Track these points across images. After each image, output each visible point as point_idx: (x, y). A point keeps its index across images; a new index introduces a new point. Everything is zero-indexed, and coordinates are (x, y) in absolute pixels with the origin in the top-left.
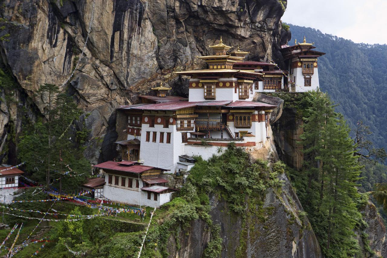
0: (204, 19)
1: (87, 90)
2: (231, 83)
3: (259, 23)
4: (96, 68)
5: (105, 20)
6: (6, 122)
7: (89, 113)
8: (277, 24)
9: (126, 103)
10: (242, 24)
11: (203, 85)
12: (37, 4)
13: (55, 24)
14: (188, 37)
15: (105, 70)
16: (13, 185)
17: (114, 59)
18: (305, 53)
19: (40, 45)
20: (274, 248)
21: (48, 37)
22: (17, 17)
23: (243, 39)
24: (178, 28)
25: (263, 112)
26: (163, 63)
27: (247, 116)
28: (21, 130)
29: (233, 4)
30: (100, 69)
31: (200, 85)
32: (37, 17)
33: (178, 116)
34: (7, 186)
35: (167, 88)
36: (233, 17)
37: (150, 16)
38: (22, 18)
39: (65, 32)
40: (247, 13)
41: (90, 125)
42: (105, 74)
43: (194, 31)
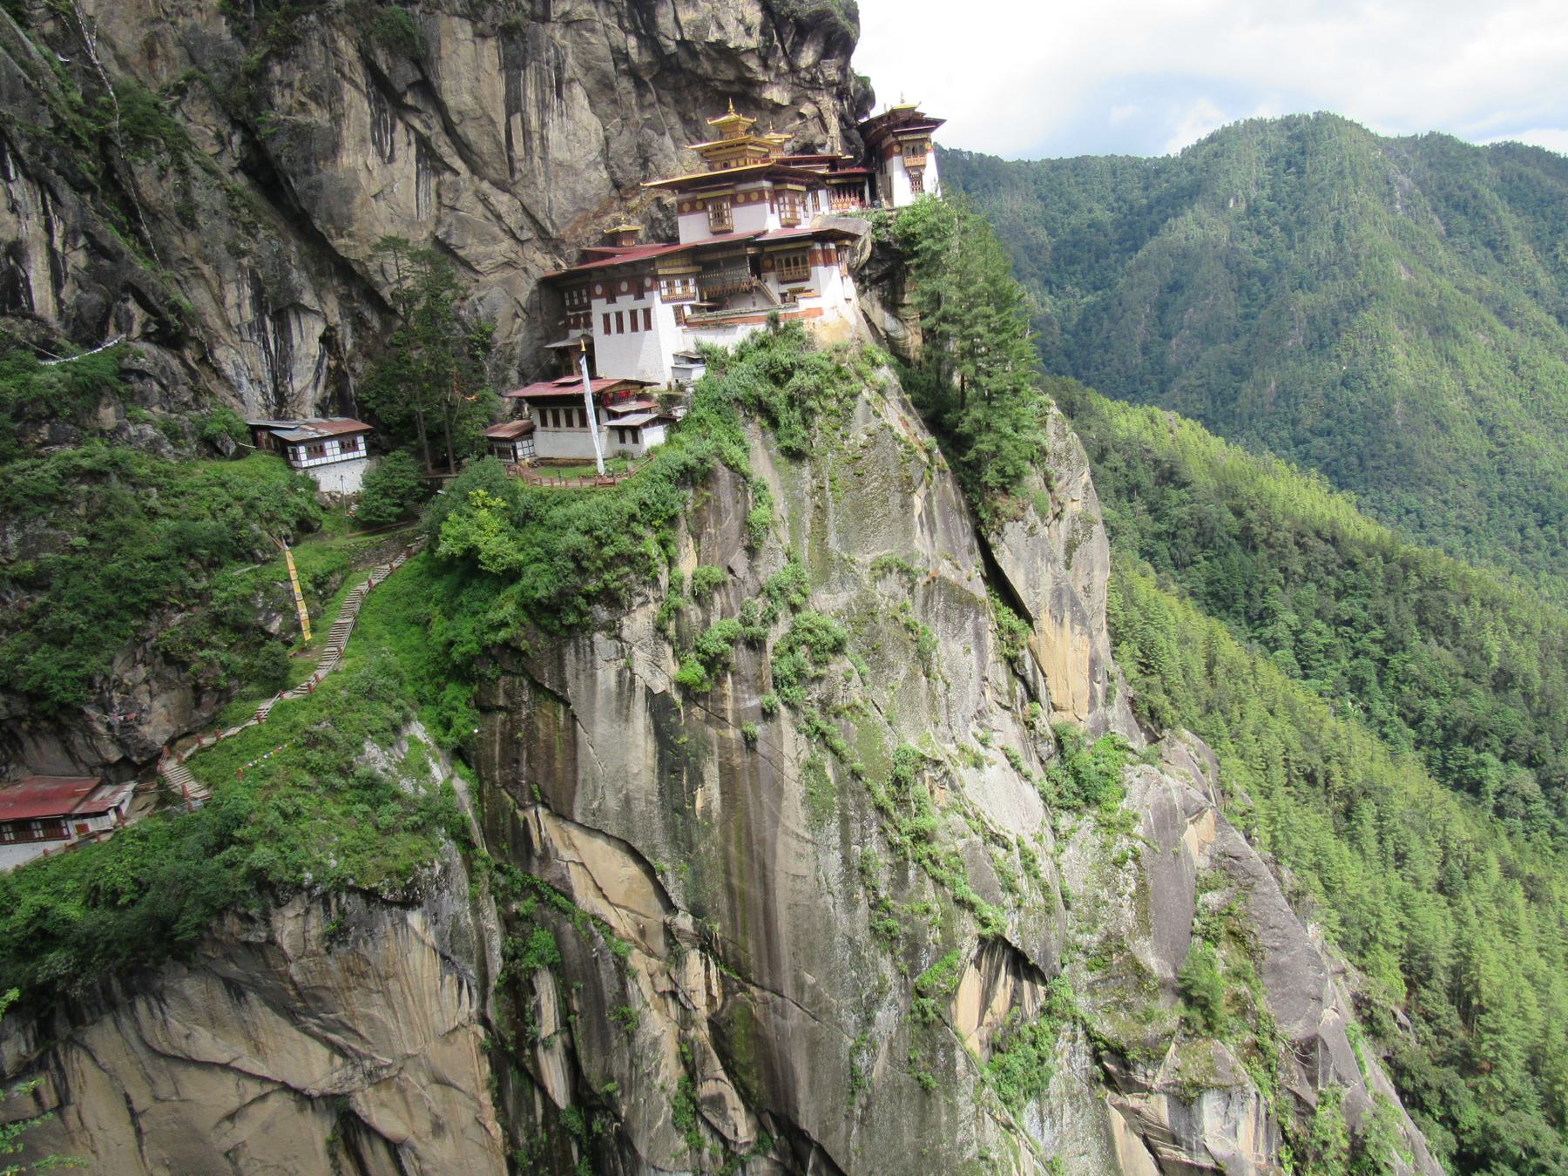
0: (693, 73)
1: (471, 248)
2: (761, 192)
3: (807, 69)
4: (485, 200)
5: (485, 91)
6: (319, 329)
7: (482, 293)
8: (844, 69)
9: (557, 266)
10: (772, 75)
11: (705, 203)
12: (339, 70)
13: (385, 111)
14: (665, 115)
15: (501, 201)
16: (356, 455)
17: (518, 176)
18: (906, 124)
19: (360, 160)
20: (880, 512)
21: (374, 143)
22: (302, 104)
23: (777, 108)
24: (640, 96)
25: (832, 246)
26: (619, 175)
27: (800, 256)
28: (355, 345)
29: (748, 31)
30: (492, 200)
31: (699, 206)
32: (342, 99)
33: (660, 272)
34: (345, 457)
35: (636, 225)
36: (753, 63)
37: (580, 73)
38: (312, 106)
39: (409, 127)
40: (780, 53)
41: (492, 319)
42: (502, 209)
43: (677, 102)
